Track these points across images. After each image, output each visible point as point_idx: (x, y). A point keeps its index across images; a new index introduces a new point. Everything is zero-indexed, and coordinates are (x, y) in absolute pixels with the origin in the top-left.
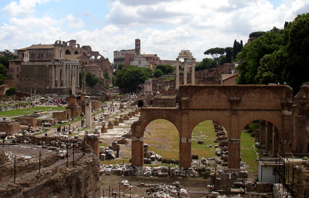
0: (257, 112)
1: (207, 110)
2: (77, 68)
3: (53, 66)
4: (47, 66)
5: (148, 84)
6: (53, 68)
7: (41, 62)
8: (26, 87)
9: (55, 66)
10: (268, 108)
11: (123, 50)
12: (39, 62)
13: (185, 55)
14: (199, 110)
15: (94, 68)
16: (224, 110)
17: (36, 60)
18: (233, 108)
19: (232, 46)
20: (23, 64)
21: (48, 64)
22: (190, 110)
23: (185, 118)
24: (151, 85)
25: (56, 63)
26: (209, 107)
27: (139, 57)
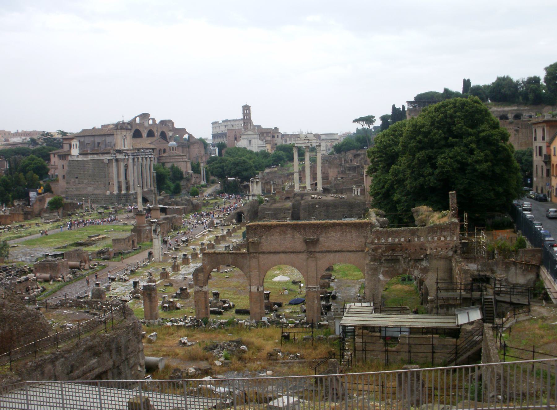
0: (337, 254)
1: (279, 253)
2: (151, 161)
3: (114, 161)
4: (106, 161)
6: (114, 164)
7: (96, 156)
8: (76, 193)
9: (117, 160)
10: (350, 250)
11: (227, 121)
12: (93, 156)
13: (307, 141)
14: (270, 253)
15: (177, 157)
16: (300, 252)
17: (89, 152)
18: (310, 250)
19: (389, 112)
20: (70, 159)
21: (106, 157)
22: (260, 253)
23: (254, 263)
24: (260, 184)
25: (119, 156)
27: (248, 134)
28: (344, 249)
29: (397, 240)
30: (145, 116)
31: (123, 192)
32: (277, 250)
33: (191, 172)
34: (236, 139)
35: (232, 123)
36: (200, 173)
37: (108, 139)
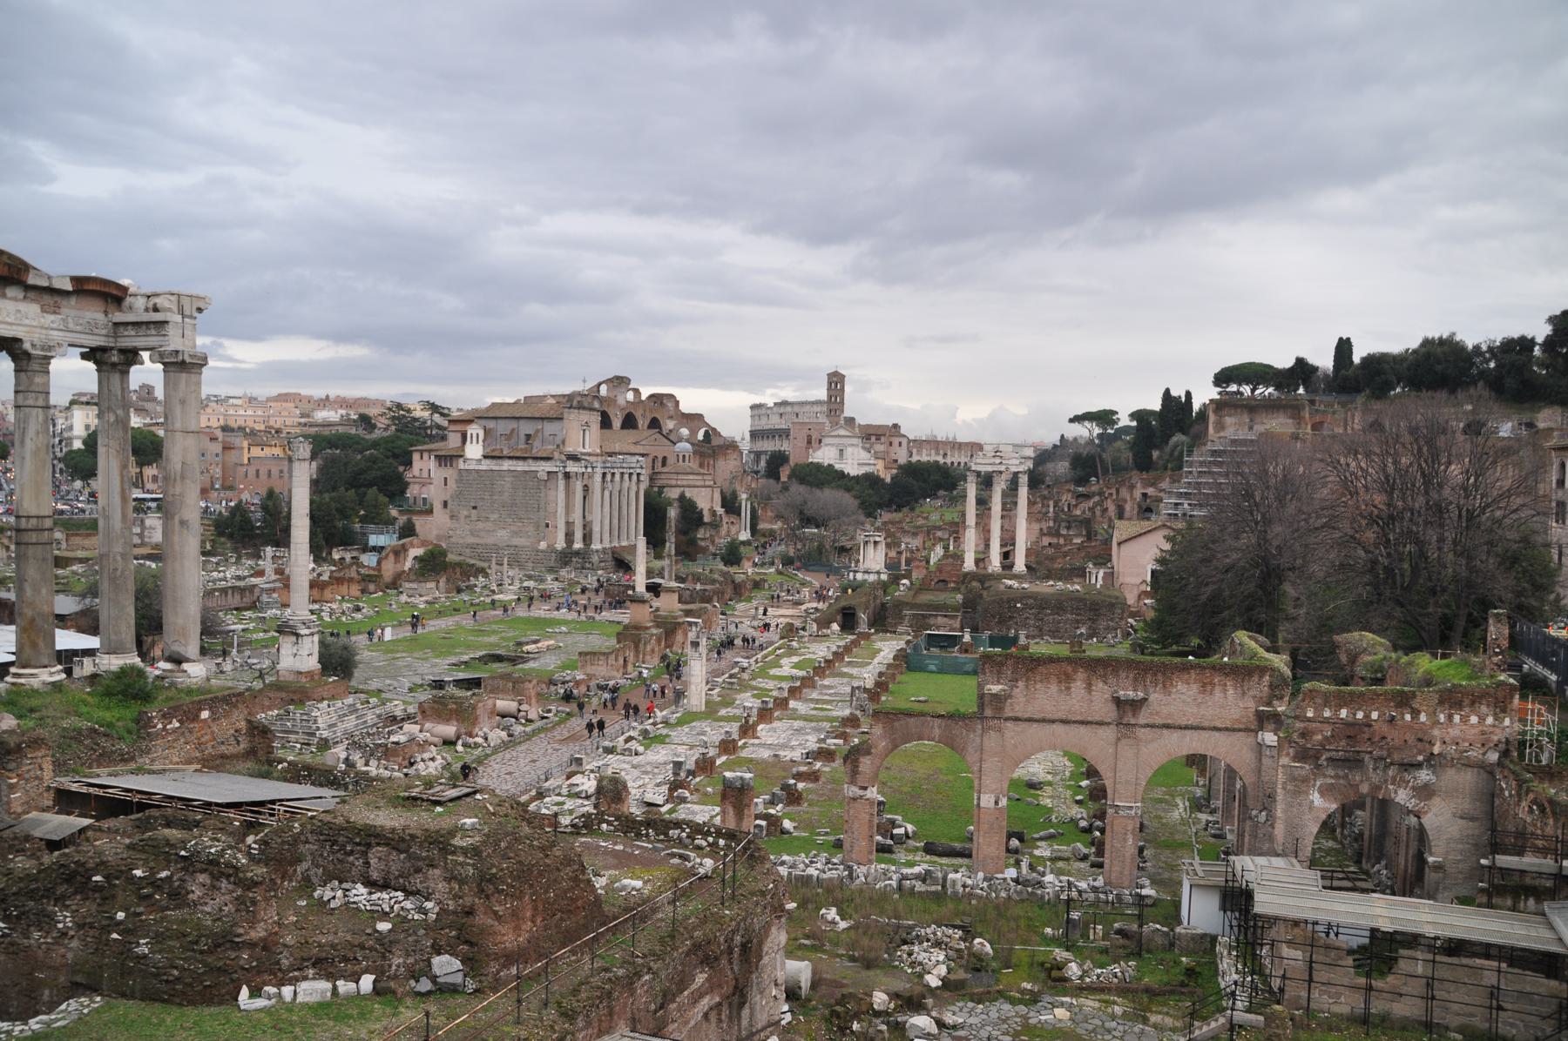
0: (1188, 732)
1: (1053, 721)
3: (560, 476)
5: (871, 547)
6: (561, 483)
7: (521, 463)
8: (471, 540)
9: (567, 476)
11: (784, 403)
16: (1100, 723)
20: (461, 465)
22: (1007, 719)
25: (572, 467)
26: (1060, 715)
28: (1206, 724)
29: (1360, 715)
30: (620, 382)
31: (578, 545)
32: (1049, 716)
33: (720, 511)
34: (809, 442)
35: (796, 409)
36: (739, 514)
37: (550, 428)
